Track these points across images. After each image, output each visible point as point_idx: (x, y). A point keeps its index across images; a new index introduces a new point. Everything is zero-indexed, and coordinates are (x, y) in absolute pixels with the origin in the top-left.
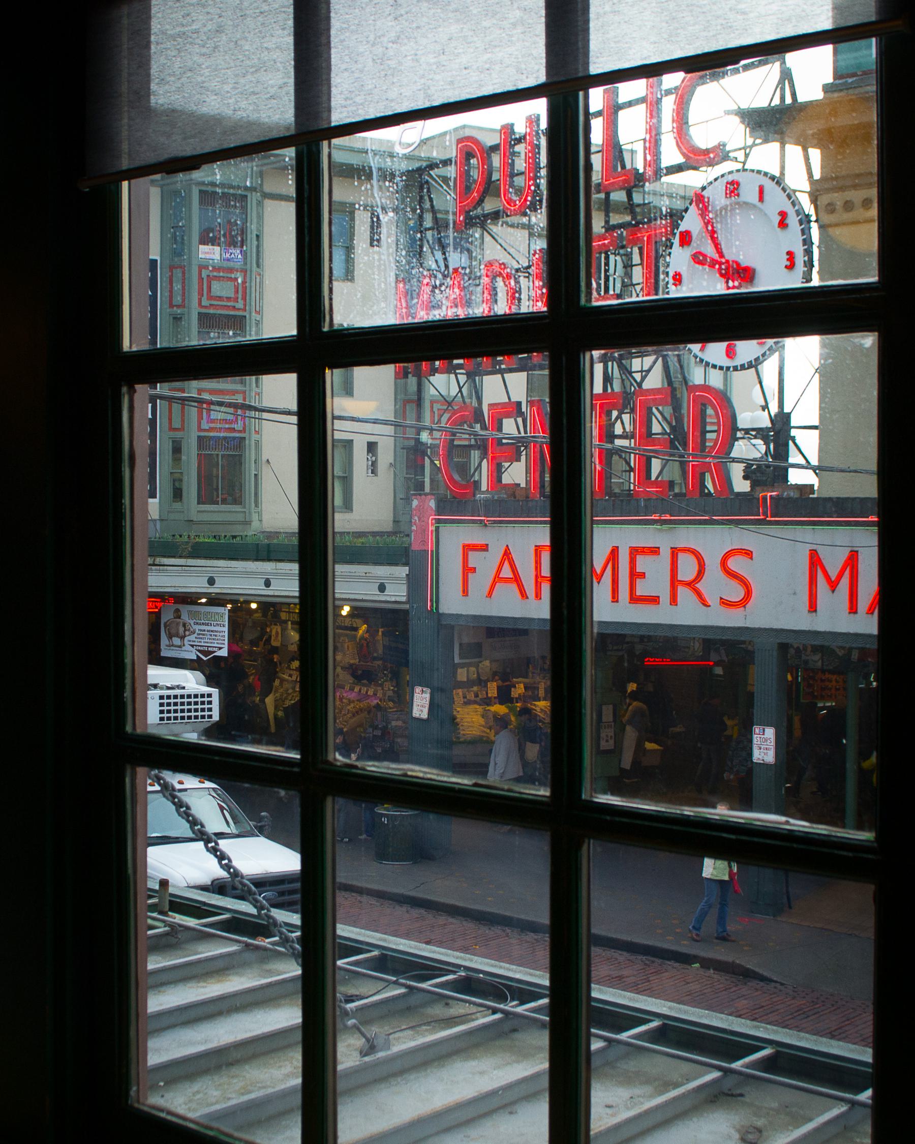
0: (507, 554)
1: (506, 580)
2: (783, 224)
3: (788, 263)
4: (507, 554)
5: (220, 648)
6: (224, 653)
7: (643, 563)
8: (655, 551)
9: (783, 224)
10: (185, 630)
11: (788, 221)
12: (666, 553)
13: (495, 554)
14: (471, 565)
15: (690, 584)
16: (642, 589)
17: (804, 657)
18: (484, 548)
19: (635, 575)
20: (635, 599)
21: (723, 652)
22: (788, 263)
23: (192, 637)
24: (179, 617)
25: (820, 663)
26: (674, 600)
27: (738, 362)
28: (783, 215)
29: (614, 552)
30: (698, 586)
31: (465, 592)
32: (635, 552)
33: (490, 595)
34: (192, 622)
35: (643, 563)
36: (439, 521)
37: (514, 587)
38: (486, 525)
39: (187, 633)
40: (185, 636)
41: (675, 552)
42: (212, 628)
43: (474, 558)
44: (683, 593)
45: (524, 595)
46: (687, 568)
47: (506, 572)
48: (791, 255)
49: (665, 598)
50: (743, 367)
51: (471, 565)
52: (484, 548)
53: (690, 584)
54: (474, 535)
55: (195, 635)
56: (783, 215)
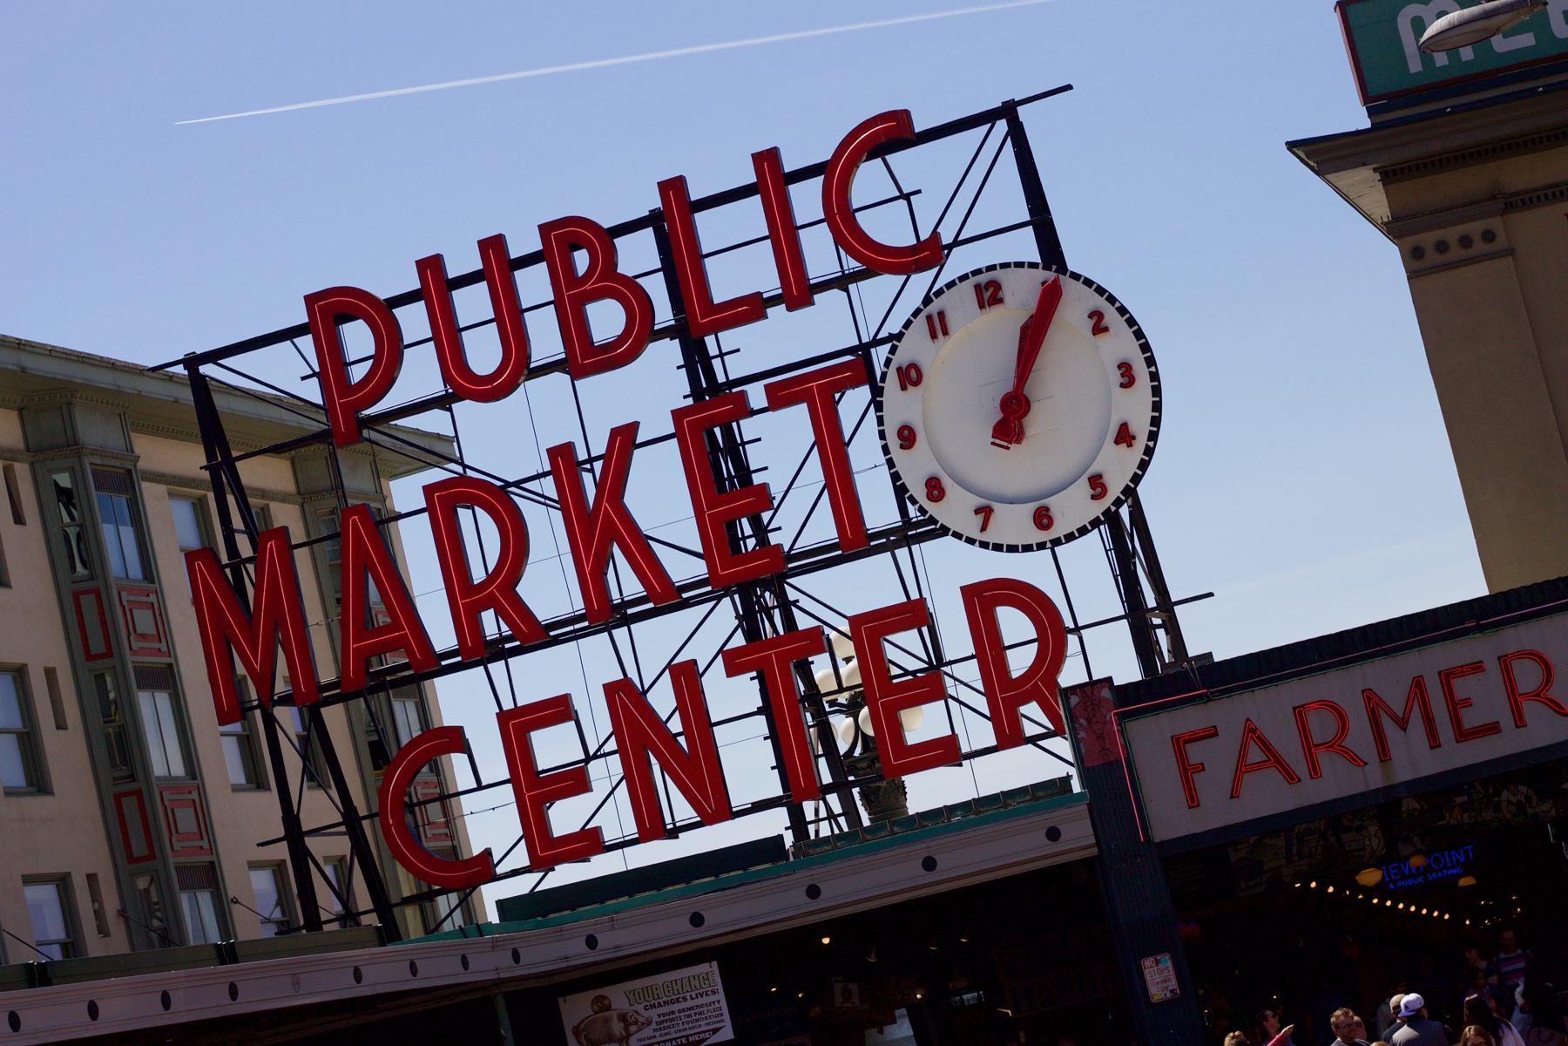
0: (1251, 731)
1: (1259, 766)
2: (1099, 328)
3: (1125, 380)
4: (1251, 731)
5: (715, 1031)
6: (727, 1034)
7: (1462, 687)
8: (1477, 667)
9: (1099, 328)
10: (627, 1025)
11: (1107, 321)
12: (1492, 667)
13: (1230, 738)
14: (1193, 760)
15: (1537, 695)
16: (1470, 719)
17: (1530, 811)
18: (1212, 733)
19: (1456, 707)
20: (1463, 735)
21: (1415, 839)
22: (1125, 380)
23: (648, 1032)
24: (609, 1008)
25: (1553, 812)
26: (1520, 721)
27: (1058, 530)
28: (1097, 315)
29: (1418, 684)
30: (1554, 692)
31: (1193, 801)
32: (1447, 677)
33: (1234, 795)
34: (640, 1008)
35: (1462, 687)
36: (1123, 717)
37: (1272, 775)
38: (1209, 700)
39: (633, 1028)
40: (629, 1035)
41: (1505, 662)
42: (690, 1003)
43: (1195, 752)
44: (1530, 709)
45: (1291, 777)
46: (1528, 676)
47: (1255, 754)
48: (1126, 369)
49: (1506, 720)
50: (1070, 537)
51: (1193, 760)
52: (1212, 733)
53: (1537, 695)
54: (1190, 718)
55: (654, 1026)
56: (1097, 315)
